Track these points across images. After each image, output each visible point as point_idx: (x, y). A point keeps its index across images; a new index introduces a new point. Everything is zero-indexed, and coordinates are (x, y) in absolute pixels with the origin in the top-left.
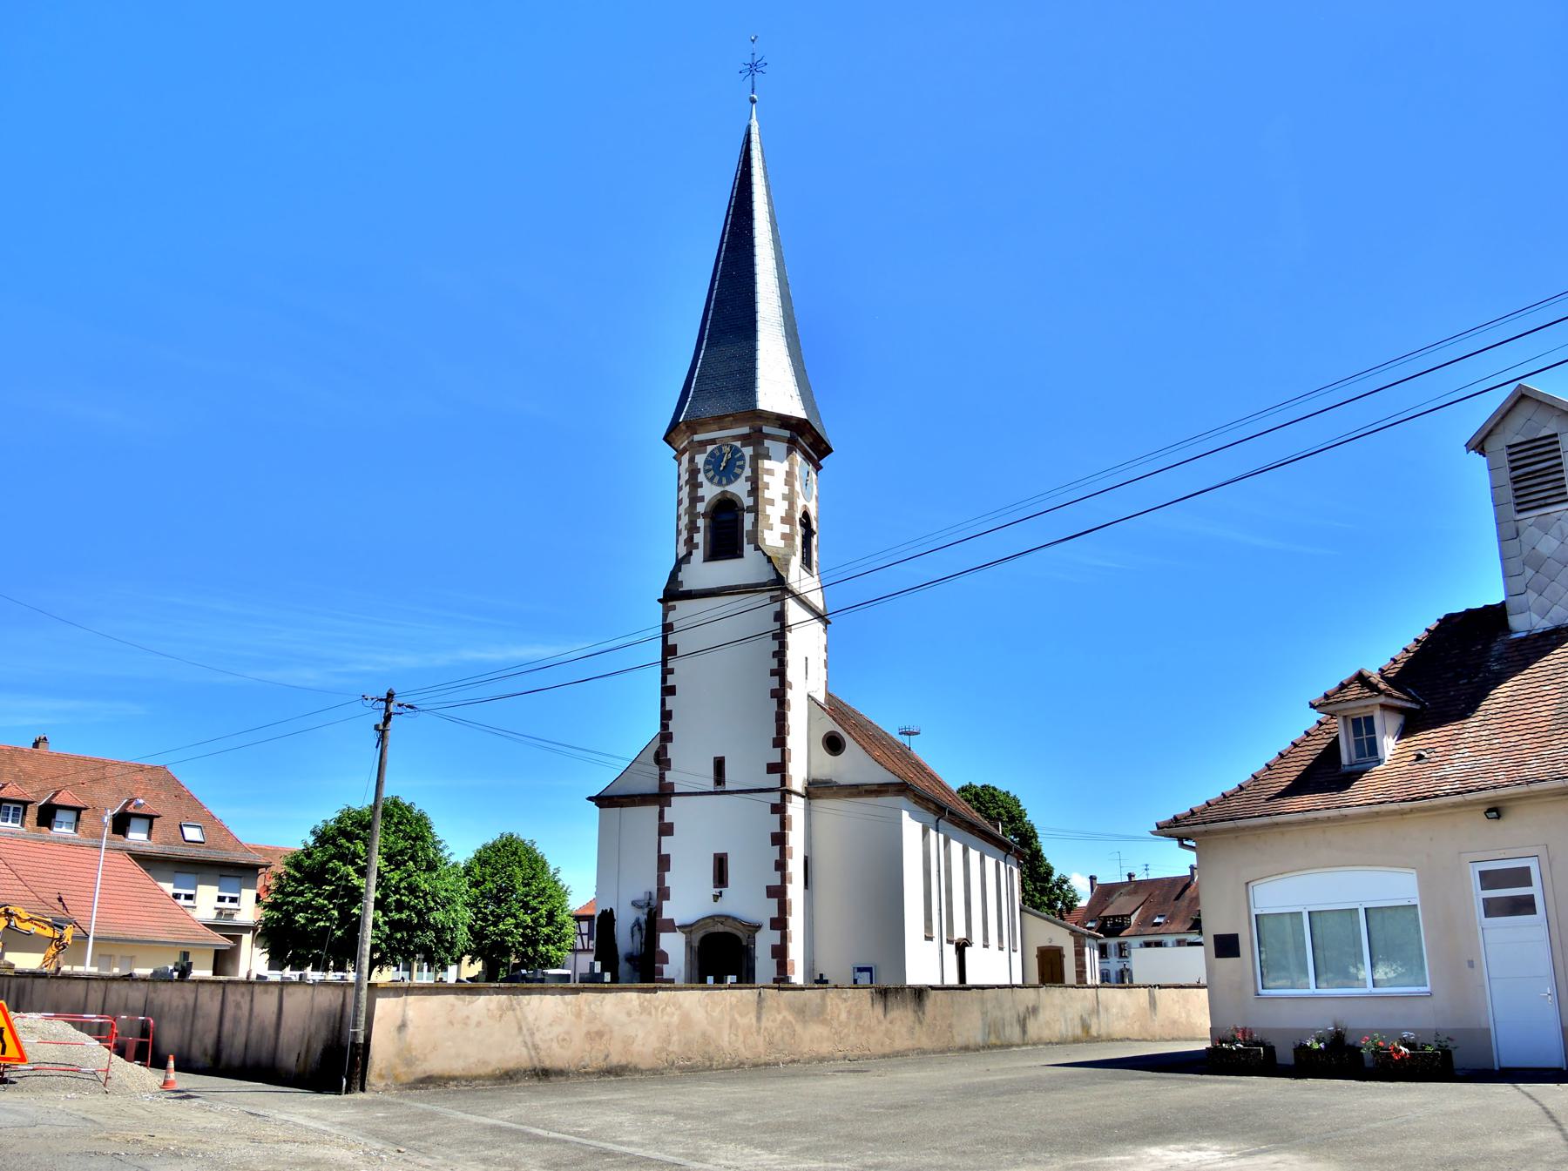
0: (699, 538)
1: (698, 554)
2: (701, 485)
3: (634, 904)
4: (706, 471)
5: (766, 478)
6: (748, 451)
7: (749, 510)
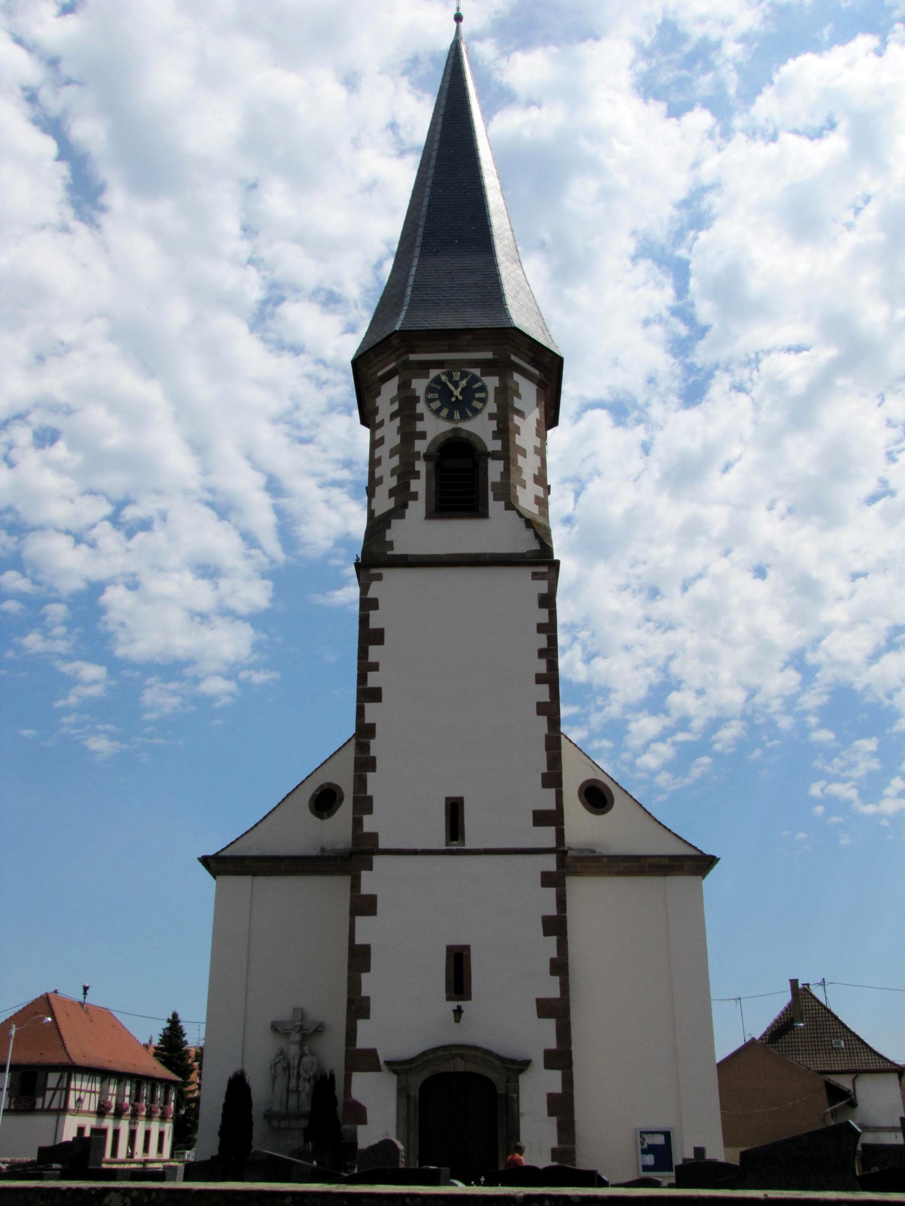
0: (418, 486)
1: (417, 509)
2: (421, 417)
3: (275, 1028)
4: (429, 401)
5: (517, 420)
6: (492, 382)
7: (495, 455)
